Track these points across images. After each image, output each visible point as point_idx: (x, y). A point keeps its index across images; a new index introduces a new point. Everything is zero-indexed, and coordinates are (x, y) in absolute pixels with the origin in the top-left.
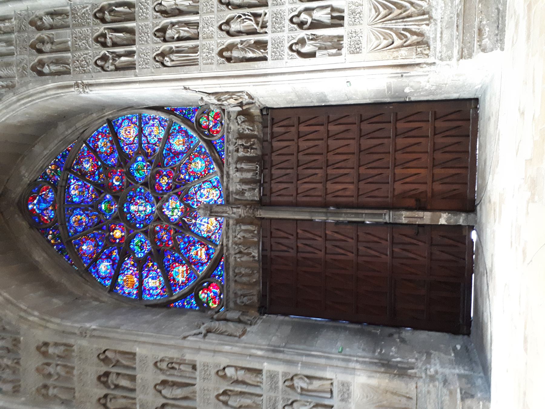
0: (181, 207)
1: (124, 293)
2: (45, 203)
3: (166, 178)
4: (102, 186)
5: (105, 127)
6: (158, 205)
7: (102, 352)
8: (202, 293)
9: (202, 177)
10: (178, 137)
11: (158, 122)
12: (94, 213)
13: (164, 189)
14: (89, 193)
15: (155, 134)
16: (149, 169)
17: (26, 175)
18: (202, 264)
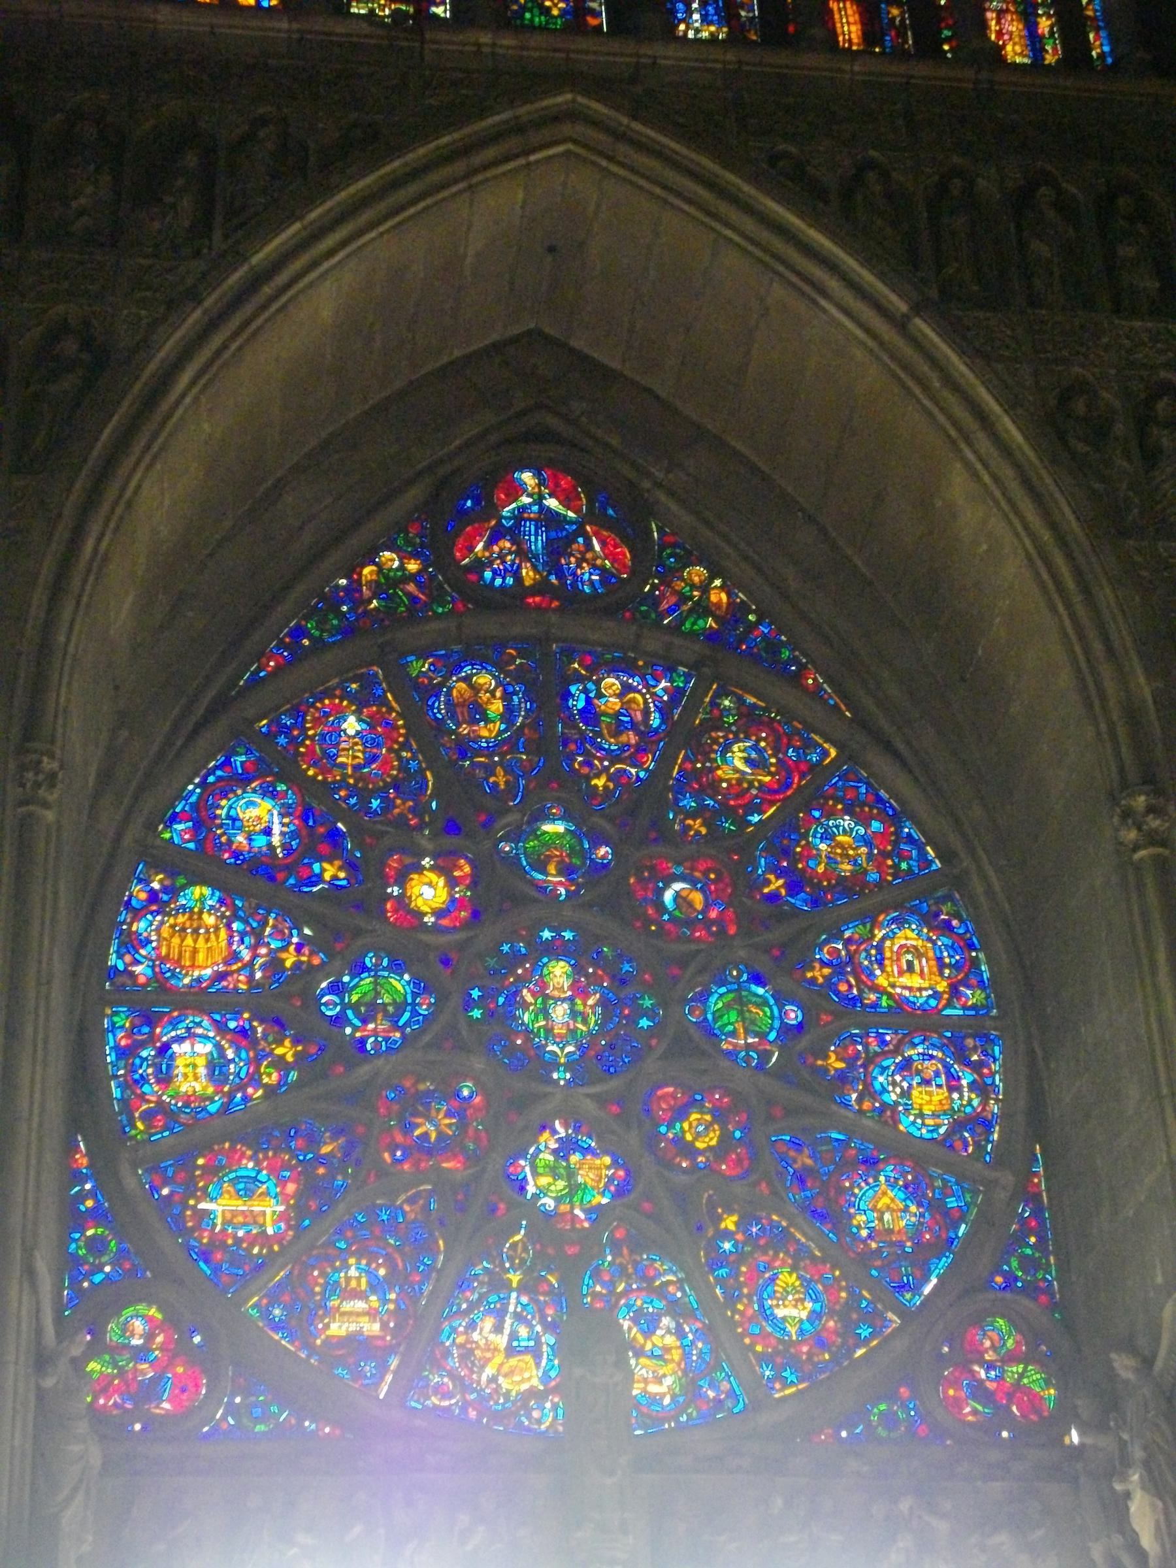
0: (577, 1212)
1: (138, 914)
3: (713, 1139)
5: (922, 854)
10: (913, 1209)
11: (968, 1110)
14: (615, 758)
15: (915, 1093)
16: (748, 1059)
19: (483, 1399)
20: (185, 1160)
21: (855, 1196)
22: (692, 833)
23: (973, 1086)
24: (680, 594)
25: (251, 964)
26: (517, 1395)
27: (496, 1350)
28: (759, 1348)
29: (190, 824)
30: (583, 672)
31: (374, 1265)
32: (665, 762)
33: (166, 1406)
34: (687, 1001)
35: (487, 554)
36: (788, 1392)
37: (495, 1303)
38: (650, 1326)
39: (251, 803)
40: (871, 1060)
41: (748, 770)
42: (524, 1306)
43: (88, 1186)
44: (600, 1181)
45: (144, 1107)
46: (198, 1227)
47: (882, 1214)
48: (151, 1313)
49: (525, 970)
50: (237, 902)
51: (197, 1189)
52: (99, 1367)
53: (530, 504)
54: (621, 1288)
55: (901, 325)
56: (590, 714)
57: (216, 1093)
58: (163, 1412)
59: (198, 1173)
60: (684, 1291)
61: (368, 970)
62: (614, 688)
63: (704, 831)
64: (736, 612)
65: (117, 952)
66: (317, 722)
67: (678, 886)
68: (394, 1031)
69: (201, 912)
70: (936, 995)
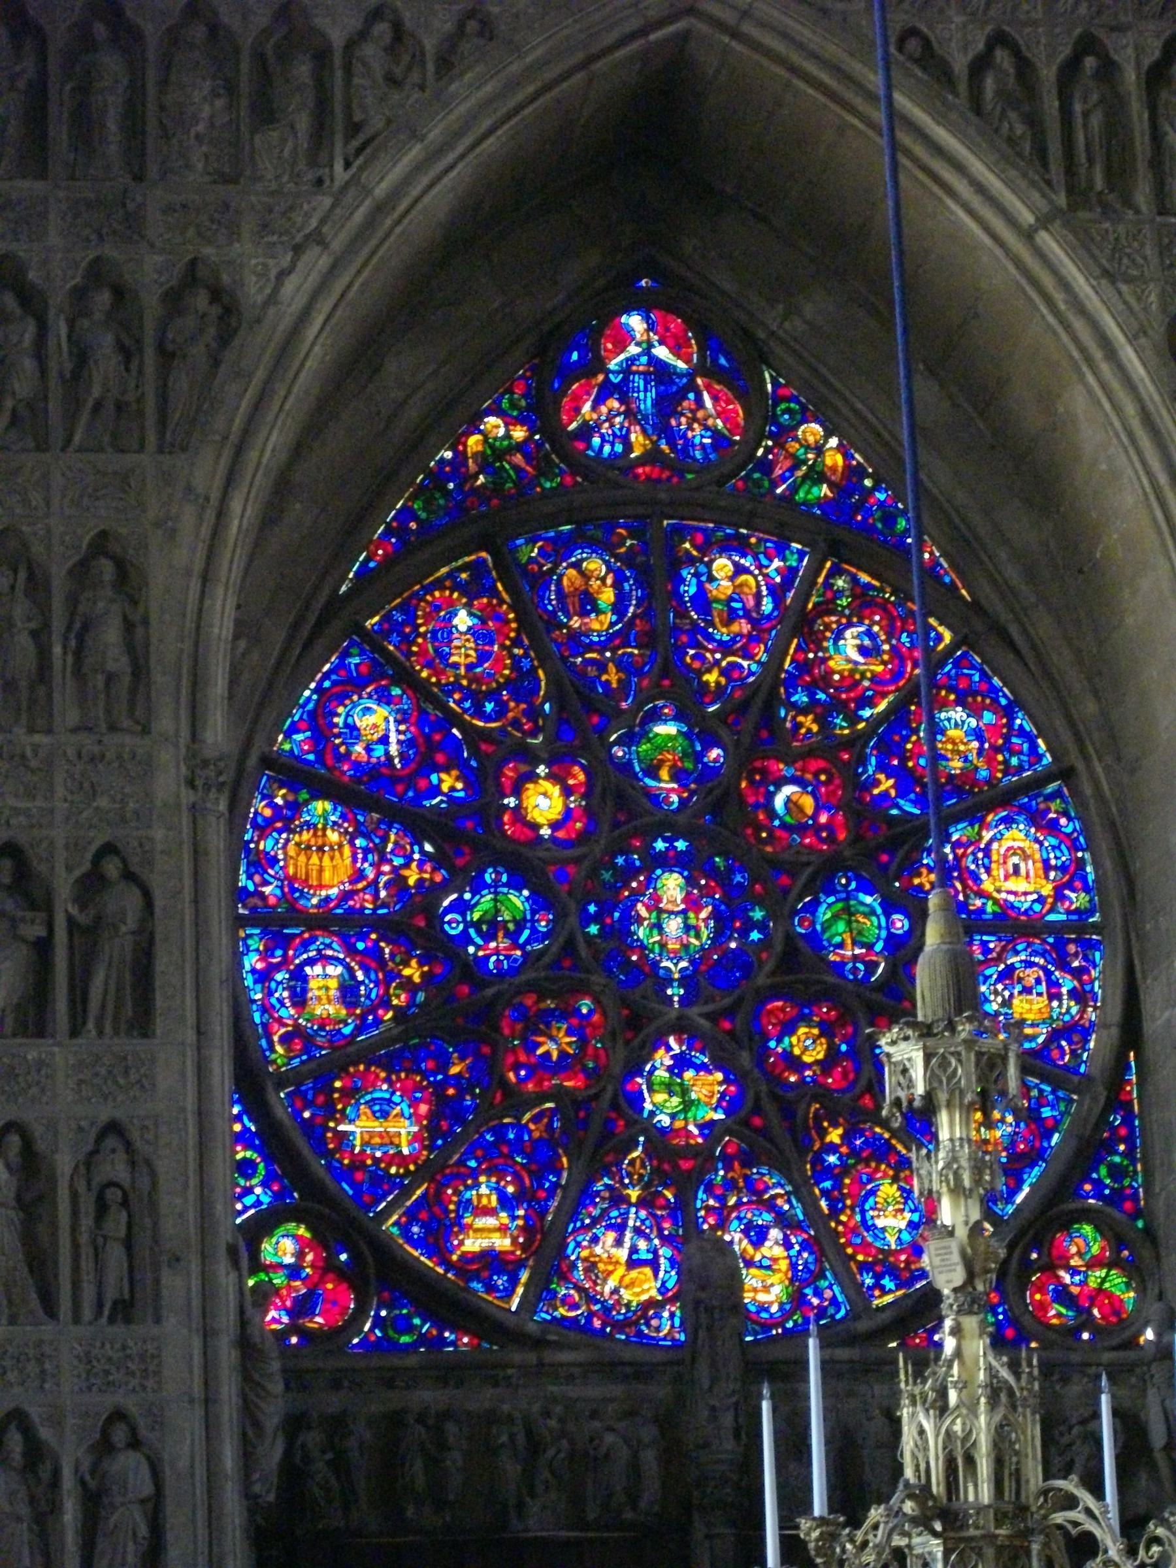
4: (769, 719)
5: (1034, 747)
6: (702, 1021)
7: (135, 869)
8: (298, 1239)
9: (838, 1235)
11: (1067, 1018)
13: (772, 1044)
15: (1016, 1002)
16: (855, 970)
17: (796, 325)
19: (607, 1310)
20: (323, 1082)
23: (1073, 993)
24: (793, 456)
25: (375, 882)
27: (617, 1263)
28: (860, 1258)
29: (308, 734)
30: (695, 553)
32: (778, 655)
33: (319, 1320)
34: (797, 912)
35: (595, 416)
38: (758, 1236)
39: (367, 710)
41: (861, 659)
42: (643, 1221)
45: (283, 1030)
46: (338, 1149)
49: (640, 882)
51: (336, 1111)
54: (732, 1201)
55: (1028, 235)
56: (702, 601)
57: (349, 1015)
59: (336, 1095)
60: (792, 1206)
61: (488, 886)
63: (815, 728)
64: (853, 473)
65: (247, 872)
66: (428, 618)
67: (788, 790)
69: (324, 829)
70: (1041, 900)
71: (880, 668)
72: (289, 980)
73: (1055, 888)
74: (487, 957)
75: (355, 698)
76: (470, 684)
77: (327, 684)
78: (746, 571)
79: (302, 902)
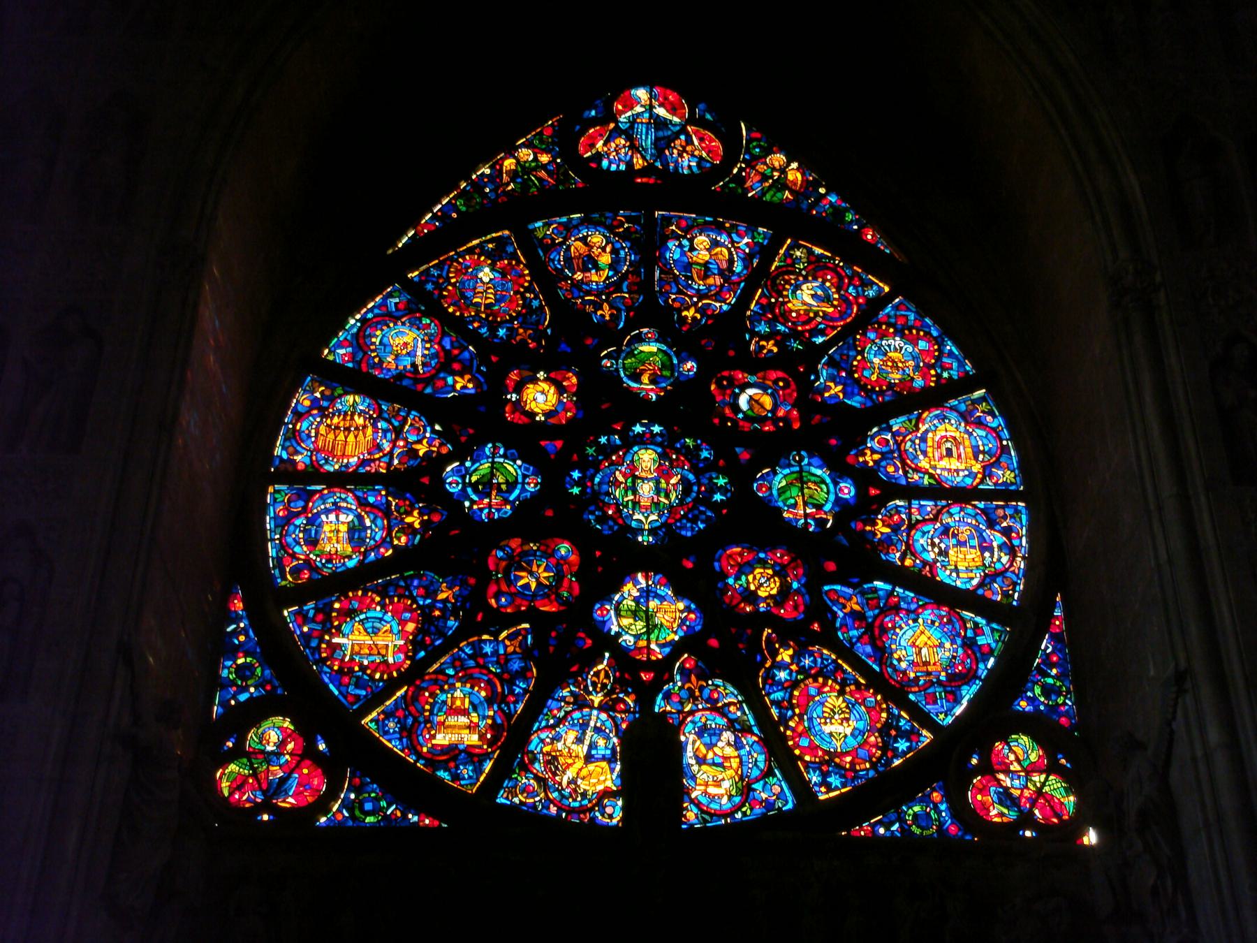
0: (653, 646)
1: (299, 416)
2: (656, 143)
10: (948, 645)
11: (998, 566)
12: (624, 314)
13: (731, 581)
14: (701, 296)
15: (951, 552)
16: (806, 524)
18: (409, 734)
21: (897, 635)
22: (765, 351)
25: (391, 453)
26: (593, 794)
27: (577, 756)
28: (807, 758)
29: (350, 350)
31: (476, 688)
33: (291, 800)
34: (757, 480)
36: (832, 794)
37: (578, 720)
39: (398, 334)
40: (912, 526)
43: (242, 625)
44: (675, 621)
47: (921, 648)
48: (285, 725)
49: (619, 456)
50: (383, 407)
51: (332, 627)
52: (238, 768)
53: (643, 112)
57: (354, 551)
58: (288, 806)
59: (334, 614)
60: (744, 713)
61: (488, 457)
62: (705, 244)
63: (775, 350)
68: (505, 505)
69: (353, 414)
71: (831, 310)
72: (306, 525)
73: (984, 467)
74: (481, 510)
75: (392, 325)
76: (487, 316)
77: (370, 316)
78: (723, 245)
79: (327, 467)
